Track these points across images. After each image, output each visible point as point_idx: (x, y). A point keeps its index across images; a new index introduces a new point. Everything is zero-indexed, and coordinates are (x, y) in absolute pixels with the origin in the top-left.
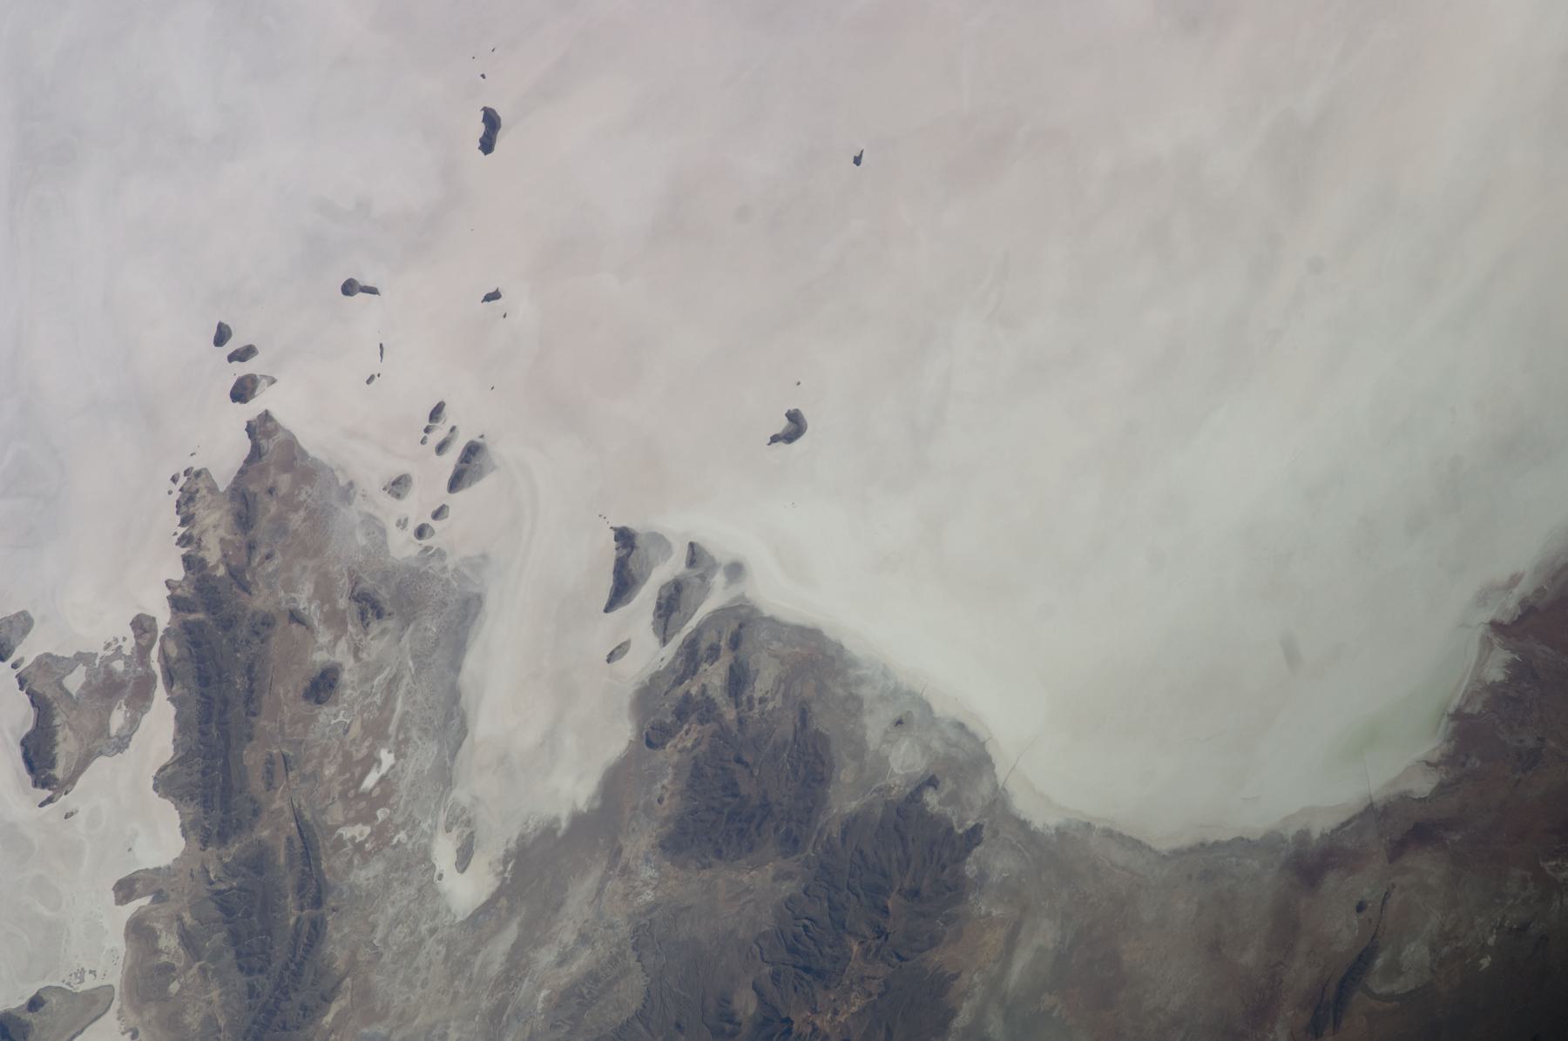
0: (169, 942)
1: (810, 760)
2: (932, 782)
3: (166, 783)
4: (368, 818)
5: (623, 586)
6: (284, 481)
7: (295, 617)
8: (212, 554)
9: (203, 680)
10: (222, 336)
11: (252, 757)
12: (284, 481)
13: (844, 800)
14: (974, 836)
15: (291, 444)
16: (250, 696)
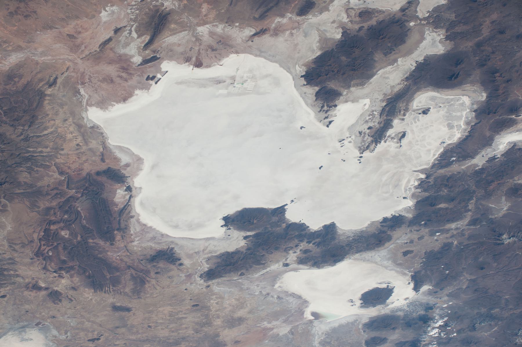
0: (402, 113)
1: (318, 95)
2: (304, 85)
3: (392, 127)
4: (373, 114)
5: (330, 122)
6: (362, 148)
7: (369, 136)
8: (374, 145)
9: (382, 134)
10: (360, 162)
11: (382, 125)
12: (362, 148)
13: (317, 89)
14: (302, 76)
15: (359, 151)
16: (378, 131)
